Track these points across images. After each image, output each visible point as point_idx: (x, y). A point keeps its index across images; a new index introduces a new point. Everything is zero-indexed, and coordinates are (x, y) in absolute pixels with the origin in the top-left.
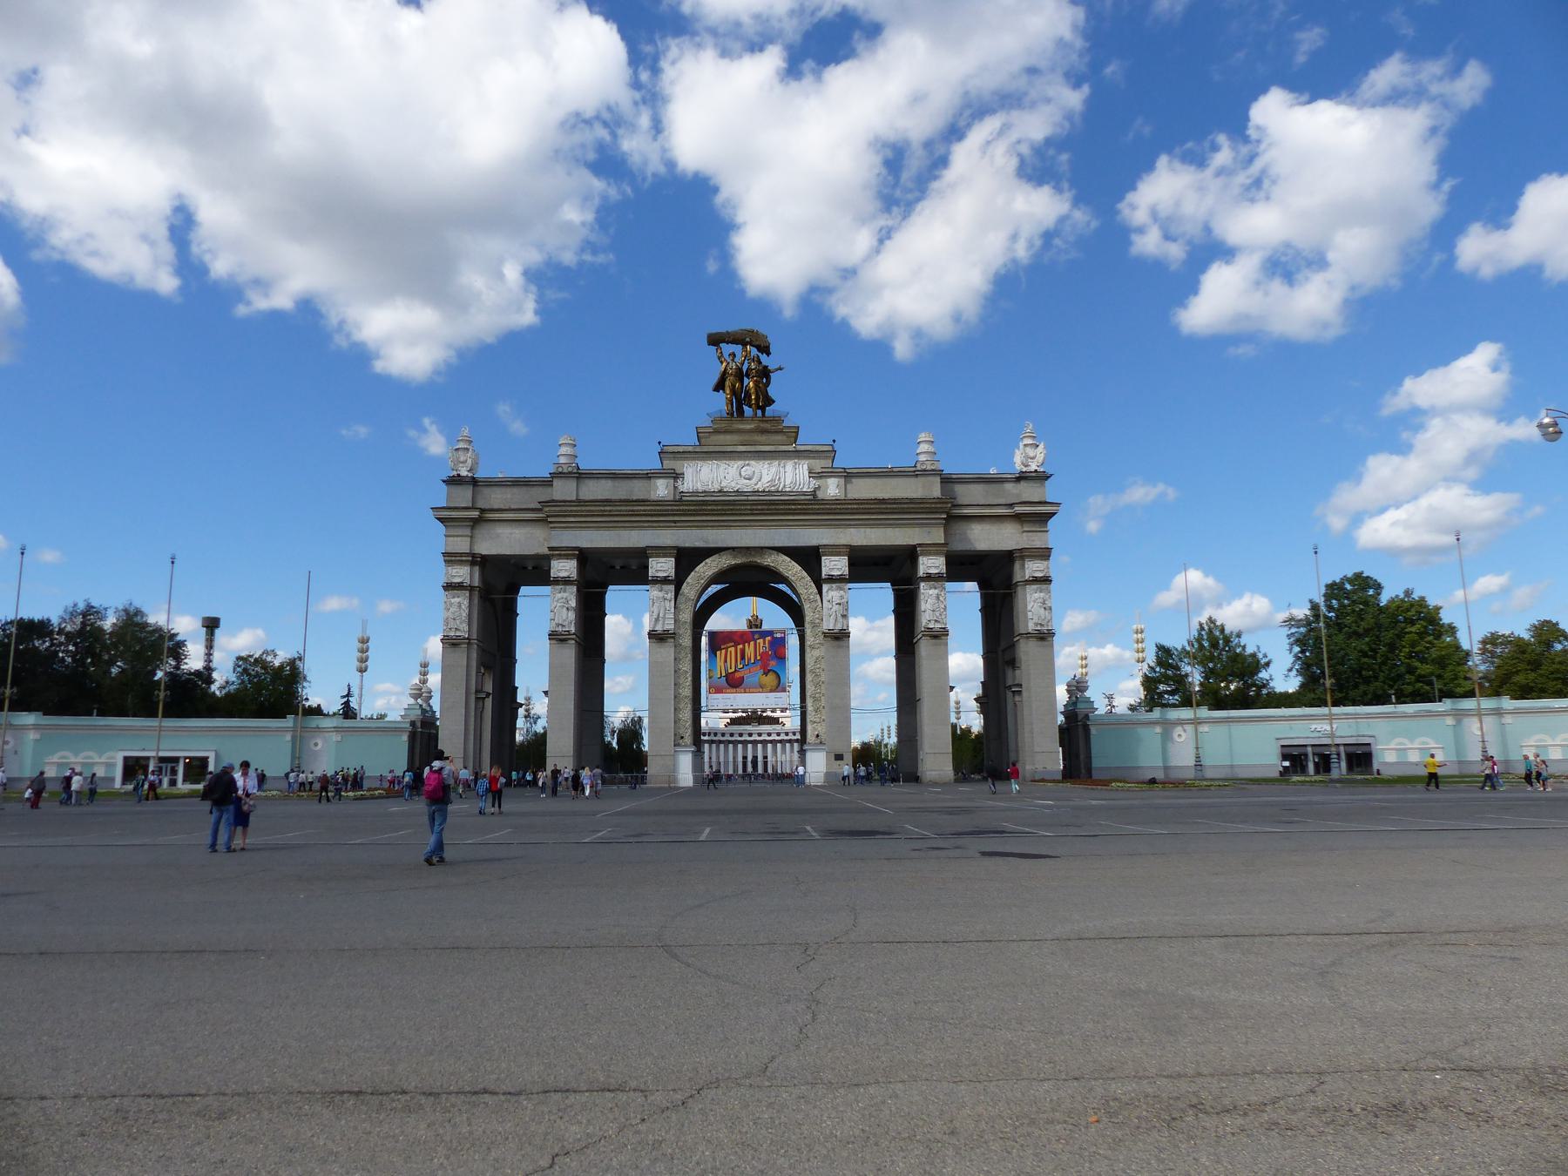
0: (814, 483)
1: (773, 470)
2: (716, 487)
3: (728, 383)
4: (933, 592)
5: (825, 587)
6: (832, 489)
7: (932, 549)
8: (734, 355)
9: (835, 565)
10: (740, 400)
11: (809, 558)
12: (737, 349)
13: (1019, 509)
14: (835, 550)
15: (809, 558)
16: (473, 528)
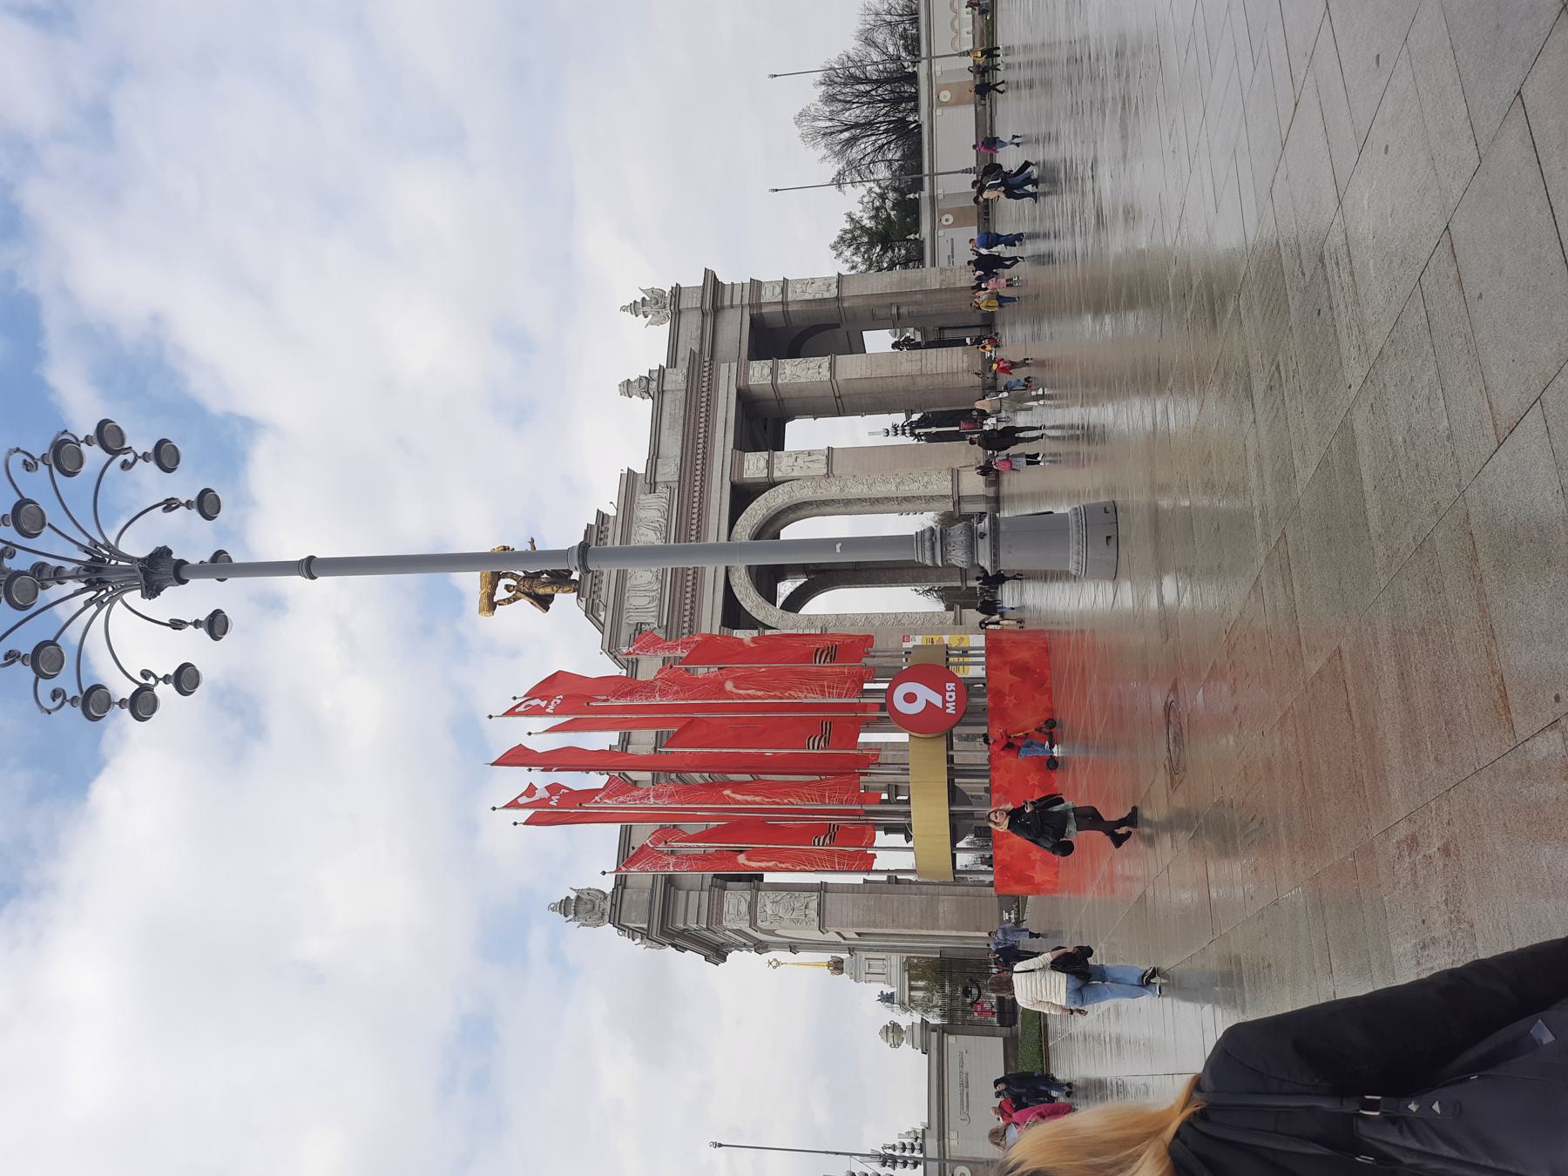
0: (659, 488)
1: (643, 530)
2: (657, 586)
3: (541, 591)
4: (788, 371)
5: (777, 474)
6: (669, 470)
7: (743, 373)
8: (507, 587)
9: (755, 466)
10: (561, 579)
11: (742, 495)
12: (502, 583)
13: (708, 305)
14: (737, 466)
15: (742, 495)
16: (678, 888)
